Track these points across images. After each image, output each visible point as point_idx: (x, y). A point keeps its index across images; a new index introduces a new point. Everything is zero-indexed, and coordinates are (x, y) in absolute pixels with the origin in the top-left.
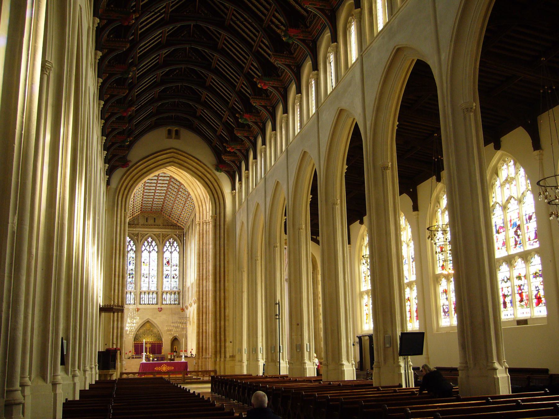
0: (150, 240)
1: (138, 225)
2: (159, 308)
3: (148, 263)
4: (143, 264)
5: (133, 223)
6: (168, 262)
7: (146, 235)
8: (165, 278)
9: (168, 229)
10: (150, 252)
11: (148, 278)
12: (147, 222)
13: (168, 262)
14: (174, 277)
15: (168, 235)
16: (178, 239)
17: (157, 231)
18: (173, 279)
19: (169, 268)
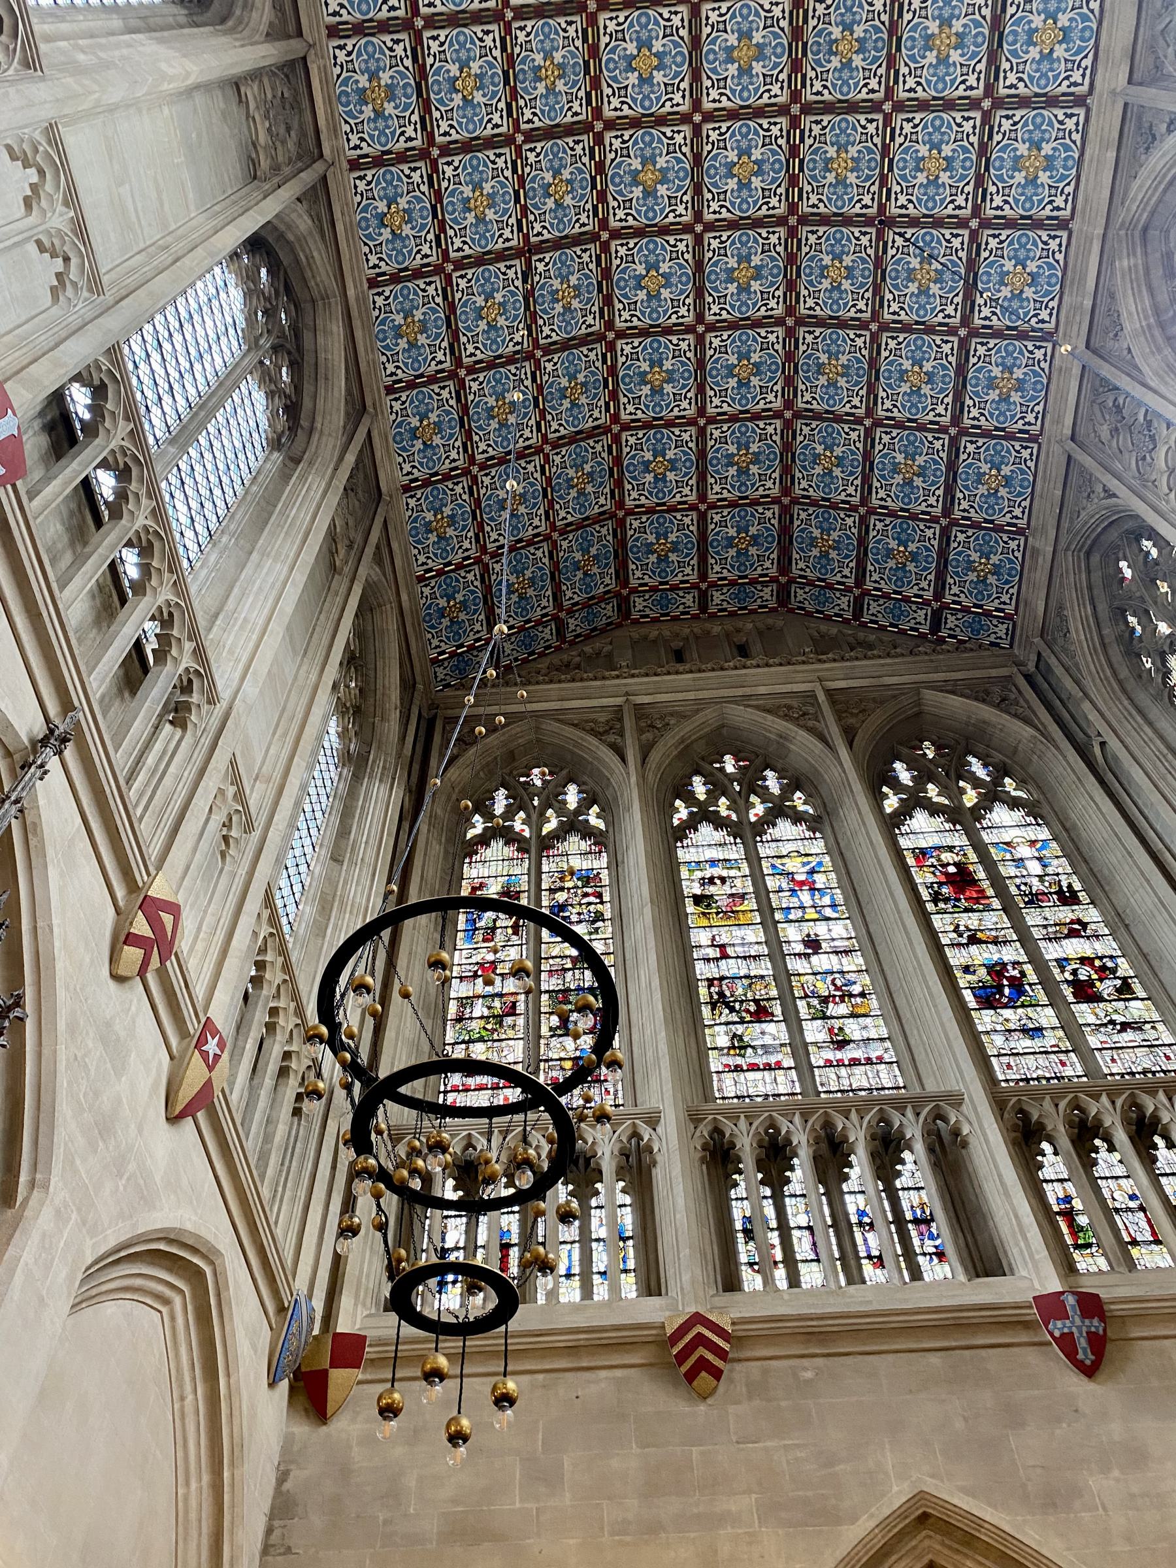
13: (962, 879)
14: (1085, 992)
18: (1085, 1013)
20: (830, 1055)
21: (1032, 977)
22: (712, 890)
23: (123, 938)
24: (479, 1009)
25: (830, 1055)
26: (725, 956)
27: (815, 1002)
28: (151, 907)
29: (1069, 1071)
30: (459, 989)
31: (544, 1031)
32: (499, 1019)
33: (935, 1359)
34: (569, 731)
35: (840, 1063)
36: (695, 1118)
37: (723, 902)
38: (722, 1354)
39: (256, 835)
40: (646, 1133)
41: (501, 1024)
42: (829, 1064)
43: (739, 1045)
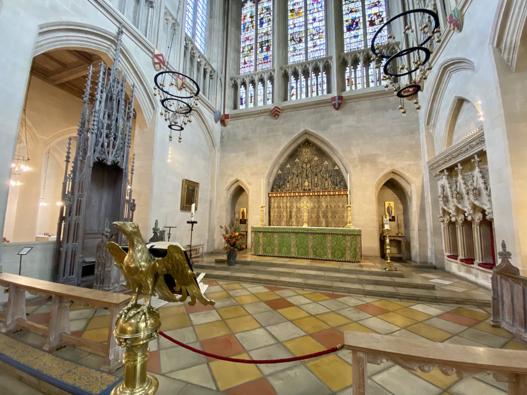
2: (333, 99)
4: (289, 14)
11: (303, 45)
14: (372, 23)
20: (312, 49)
21: (361, 21)
22: (295, 7)
23: (155, 64)
24: (246, 49)
25: (312, 49)
26: (295, 27)
27: (312, 36)
28: (156, 56)
29: (360, 46)
30: (243, 45)
31: (258, 52)
32: (250, 50)
33: (313, 110)
35: (314, 51)
36: (281, 69)
37: (296, 10)
38: (279, 112)
39: (180, 26)
40: (273, 73)
41: (250, 52)
42: (312, 52)
43: (295, 50)
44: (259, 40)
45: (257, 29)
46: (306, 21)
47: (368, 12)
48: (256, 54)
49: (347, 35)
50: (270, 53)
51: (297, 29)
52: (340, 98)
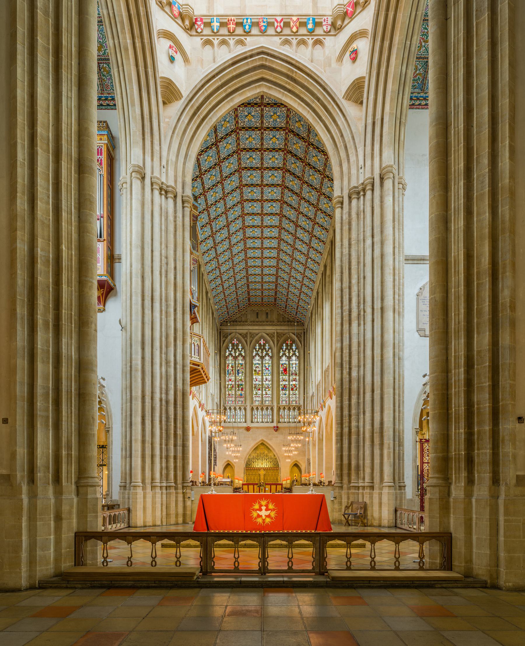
0: (262, 342)
1: (246, 322)
2: (274, 427)
3: (260, 372)
5: (240, 320)
6: (285, 370)
7: (257, 335)
8: (282, 390)
9: (284, 325)
10: (262, 358)
12: (257, 318)
14: (292, 389)
15: (284, 335)
16: (296, 339)
17: (270, 329)
18: (291, 392)
19: (286, 377)
30: (227, 383)
34: (240, 336)
44: (237, 383)
45: (235, 376)
46: (262, 379)
47: (291, 383)
48: (236, 391)
49: (281, 392)
50: (243, 392)
51: (257, 382)
52: (277, 427)
